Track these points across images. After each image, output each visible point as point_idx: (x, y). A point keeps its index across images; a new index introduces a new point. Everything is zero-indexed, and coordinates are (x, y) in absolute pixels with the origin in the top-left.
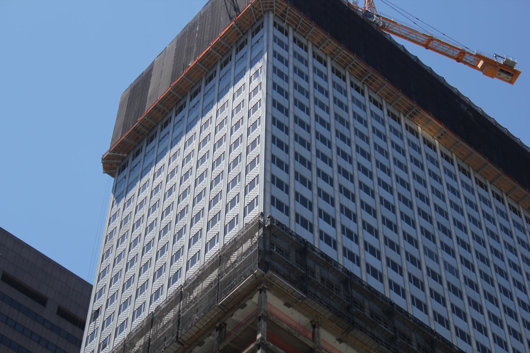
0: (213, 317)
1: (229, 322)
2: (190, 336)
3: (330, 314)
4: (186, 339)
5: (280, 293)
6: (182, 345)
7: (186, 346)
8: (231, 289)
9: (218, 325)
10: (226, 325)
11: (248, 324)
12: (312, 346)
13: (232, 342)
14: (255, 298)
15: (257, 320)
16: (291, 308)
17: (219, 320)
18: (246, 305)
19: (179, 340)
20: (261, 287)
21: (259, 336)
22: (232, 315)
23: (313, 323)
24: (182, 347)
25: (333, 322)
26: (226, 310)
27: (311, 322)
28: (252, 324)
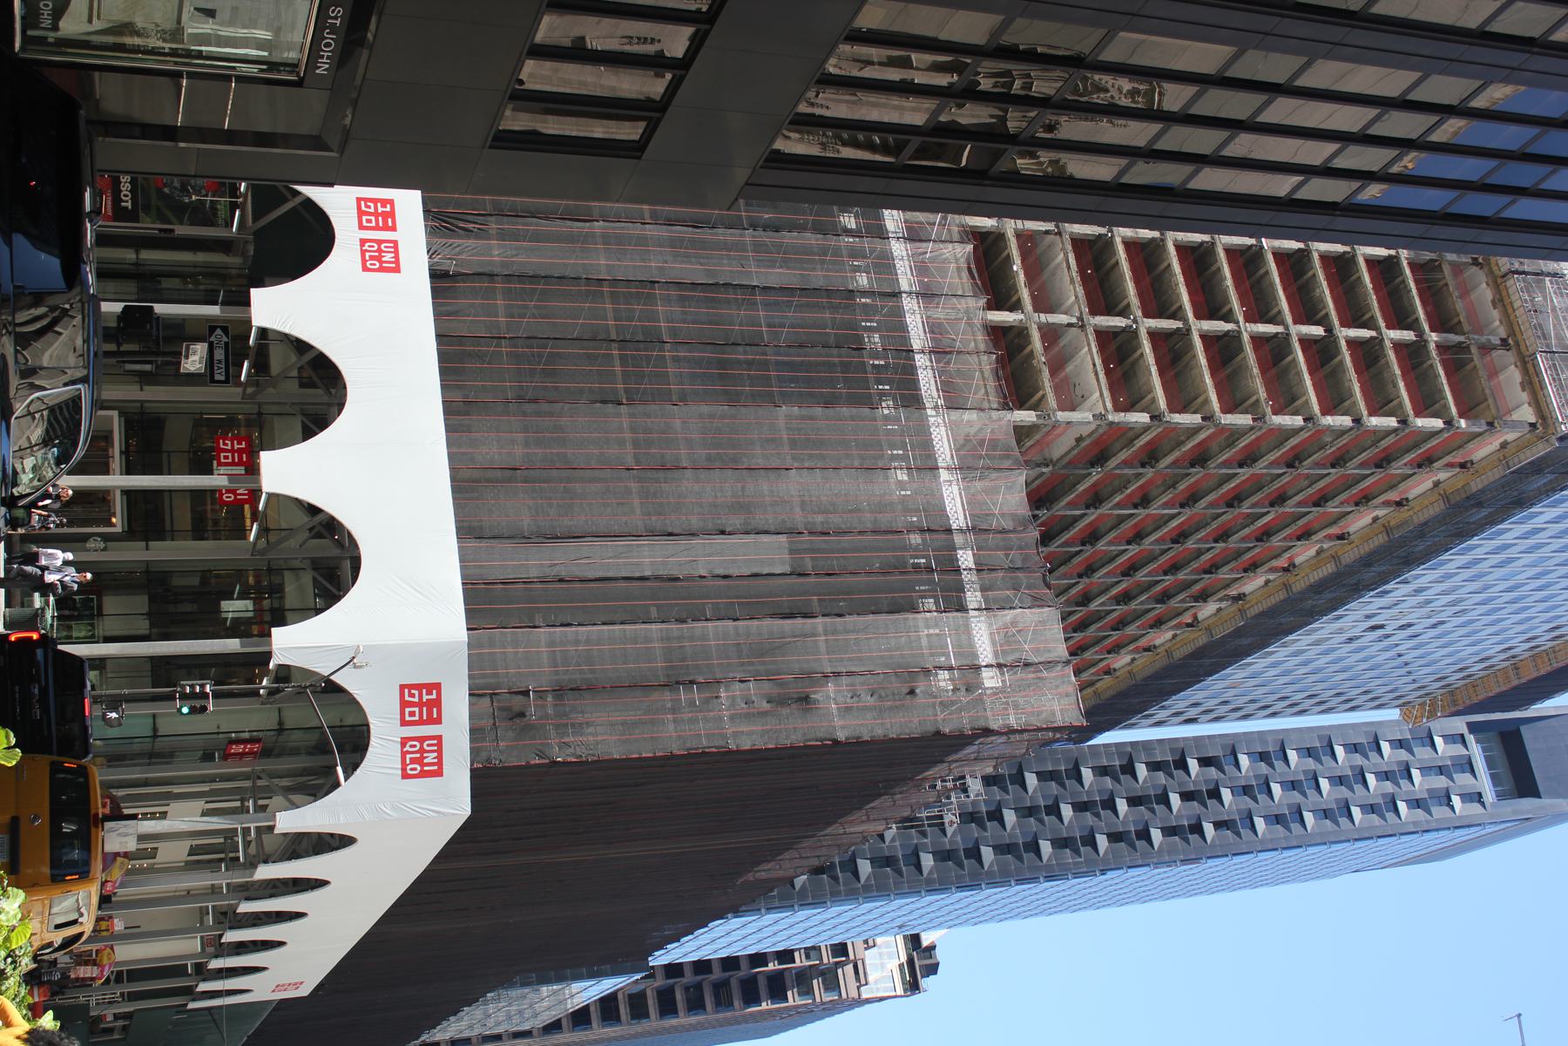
0: (1525, 336)
1: (1509, 357)
2: (1511, 291)
3: (1474, 489)
4: (1508, 284)
5: (1522, 446)
6: (1503, 276)
7: (1499, 281)
8: (1554, 379)
9: (1510, 341)
10: (1508, 350)
11: (1490, 401)
12: (1434, 465)
13: (1475, 367)
14: (1527, 414)
15: (1489, 420)
16: (1498, 447)
17: (1517, 344)
18: (1523, 390)
19: (1510, 276)
20: (1538, 425)
21: (1463, 423)
22: (1516, 366)
23: (1469, 465)
24: (1501, 274)
25: (1463, 487)
26: (1526, 359)
27: (1472, 463)
28: (1489, 406)
